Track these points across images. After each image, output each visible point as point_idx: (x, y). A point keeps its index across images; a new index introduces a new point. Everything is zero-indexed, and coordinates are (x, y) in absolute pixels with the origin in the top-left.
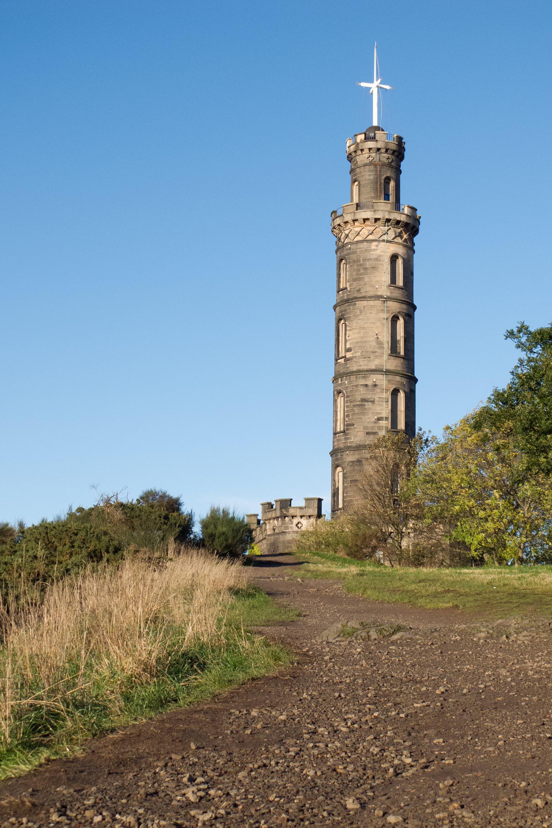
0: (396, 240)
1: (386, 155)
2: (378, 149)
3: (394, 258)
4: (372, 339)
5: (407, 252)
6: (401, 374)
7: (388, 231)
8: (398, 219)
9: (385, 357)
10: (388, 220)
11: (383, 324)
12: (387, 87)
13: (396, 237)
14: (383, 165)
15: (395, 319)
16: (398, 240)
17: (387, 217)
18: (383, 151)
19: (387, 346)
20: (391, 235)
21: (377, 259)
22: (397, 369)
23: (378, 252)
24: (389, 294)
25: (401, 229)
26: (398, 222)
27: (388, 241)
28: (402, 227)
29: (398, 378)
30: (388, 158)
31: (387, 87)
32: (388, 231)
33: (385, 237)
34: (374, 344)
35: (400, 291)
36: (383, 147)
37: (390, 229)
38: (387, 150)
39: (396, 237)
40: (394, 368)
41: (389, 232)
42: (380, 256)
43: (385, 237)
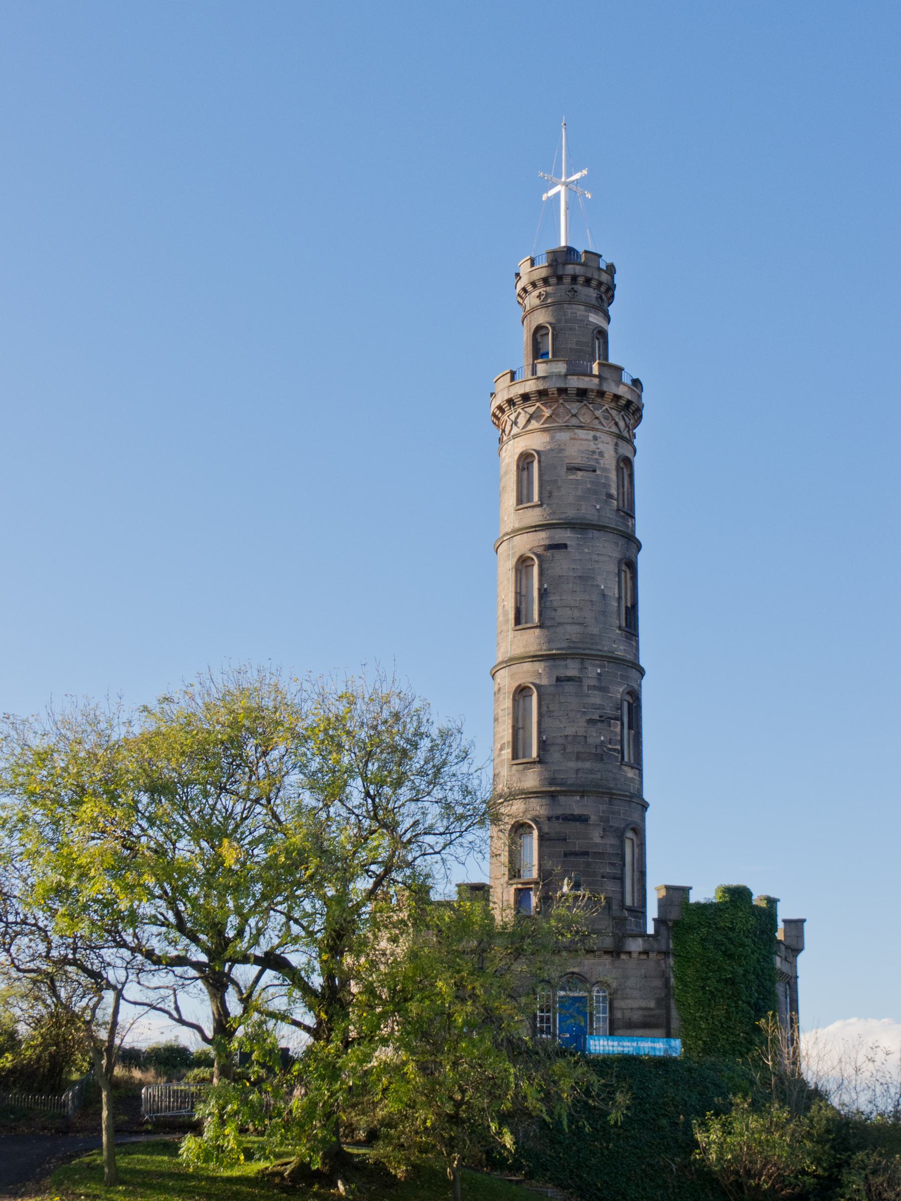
0: (530, 427)
1: (536, 293)
2: (524, 290)
3: (525, 461)
4: (500, 610)
5: (552, 438)
6: (533, 657)
7: (517, 418)
8: (522, 392)
9: (511, 634)
10: (511, 402)
11: (508, 579)
12: (576, 176)
13: (529, 421)
14: (533, 309)
15: (523, 564)
16: (534, 424)
17: (506, 398)
18: (530, 288)
19: (512, 616)
20: (522, 421)
21: (506, 473)
22: (528, 650)
23: (507, 461)
24: (517, 526)
25: (538, 404)
26: (525, 397)
27: (515, 436)
28: (538, 401)
29: (527, 666)
30: (539, 297)
31: (576, 176)
32: (517, 418)
33: (515, 430)
34: (501, 618)
35: (538, 511)
36: (526, 282)
37: (519, 413)
38: (534, 285)
39: (529, 421)
40: (523, 651)
41: (518, 420)
42: (508, 464)
43: (515, 430)
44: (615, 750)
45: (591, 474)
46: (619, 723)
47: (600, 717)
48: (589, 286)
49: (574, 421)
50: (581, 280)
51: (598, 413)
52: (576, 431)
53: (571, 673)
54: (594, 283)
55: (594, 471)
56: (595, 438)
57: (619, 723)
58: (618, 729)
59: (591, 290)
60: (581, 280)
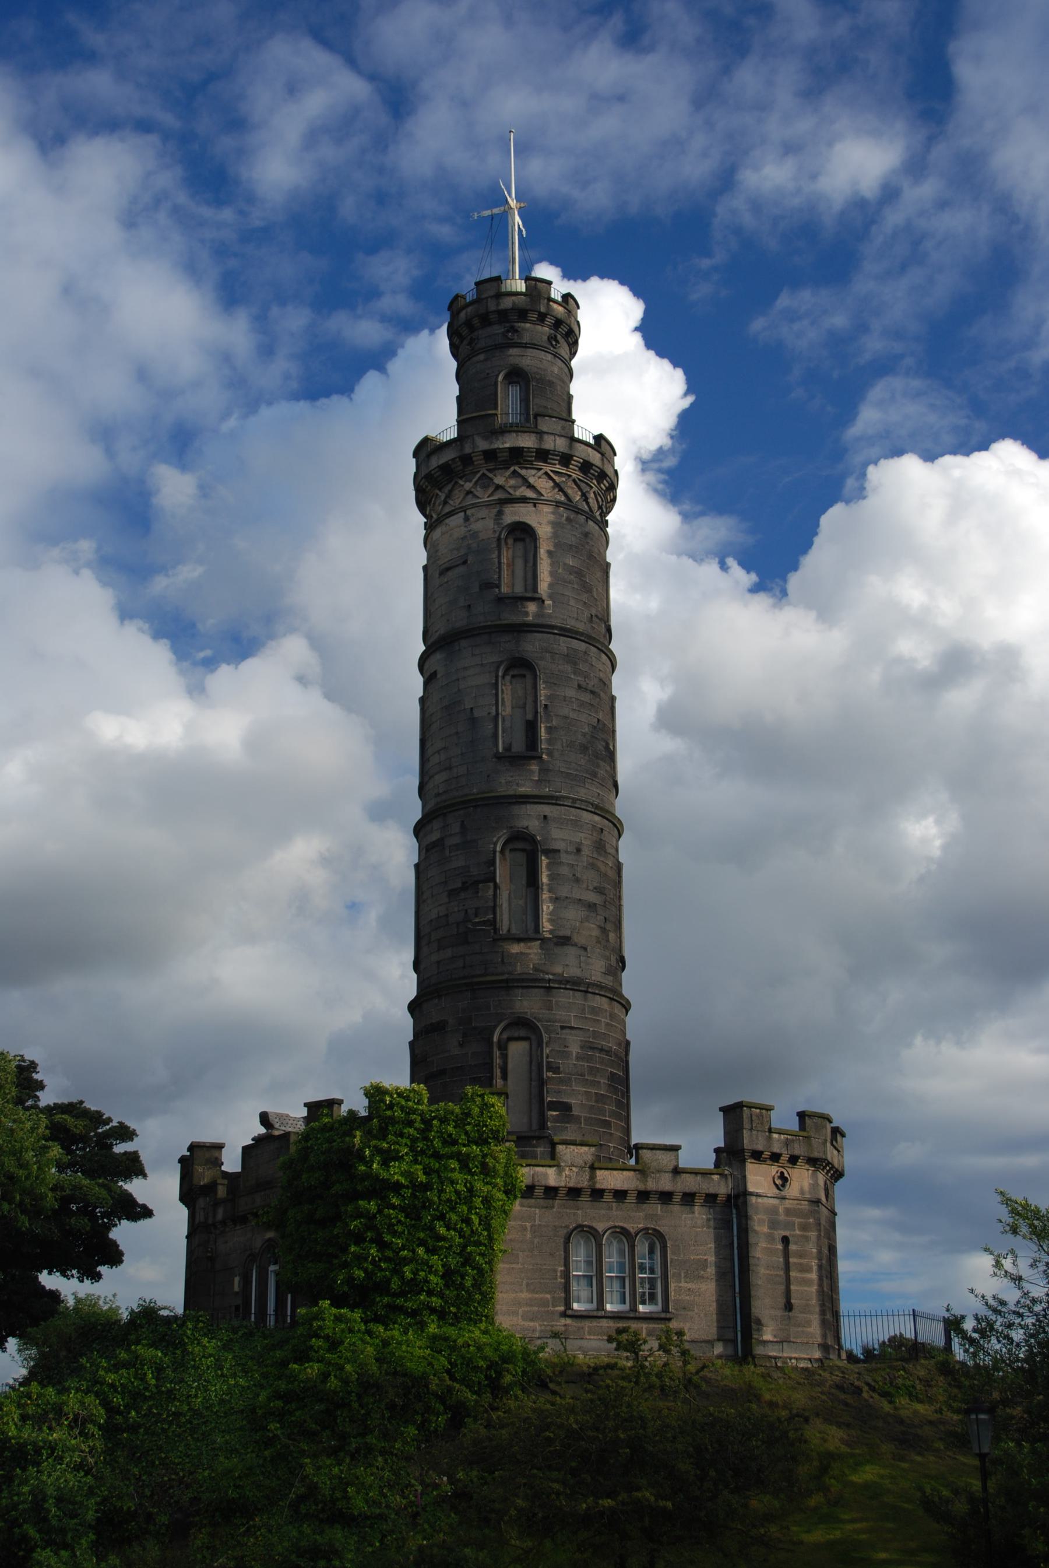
44: (484, 923)
45: (462, 569)
46: (491, 884)
47: (463, 883)
48: (490, 324)
49: (447, 509)
50: (476, 322)
51: (468, 486)
52: (447, 521)
53: (435, 836)
54: (493, 317)
55: (465, 562)
56: (467, 519)
57: (491, 884)
58: (491, 892)
59: (496, 327)
60: (476, 322)
